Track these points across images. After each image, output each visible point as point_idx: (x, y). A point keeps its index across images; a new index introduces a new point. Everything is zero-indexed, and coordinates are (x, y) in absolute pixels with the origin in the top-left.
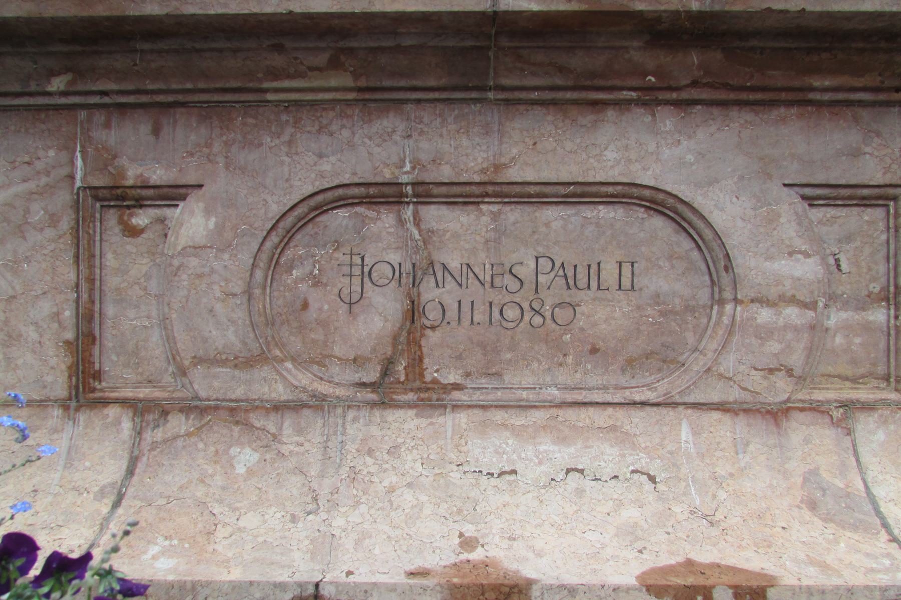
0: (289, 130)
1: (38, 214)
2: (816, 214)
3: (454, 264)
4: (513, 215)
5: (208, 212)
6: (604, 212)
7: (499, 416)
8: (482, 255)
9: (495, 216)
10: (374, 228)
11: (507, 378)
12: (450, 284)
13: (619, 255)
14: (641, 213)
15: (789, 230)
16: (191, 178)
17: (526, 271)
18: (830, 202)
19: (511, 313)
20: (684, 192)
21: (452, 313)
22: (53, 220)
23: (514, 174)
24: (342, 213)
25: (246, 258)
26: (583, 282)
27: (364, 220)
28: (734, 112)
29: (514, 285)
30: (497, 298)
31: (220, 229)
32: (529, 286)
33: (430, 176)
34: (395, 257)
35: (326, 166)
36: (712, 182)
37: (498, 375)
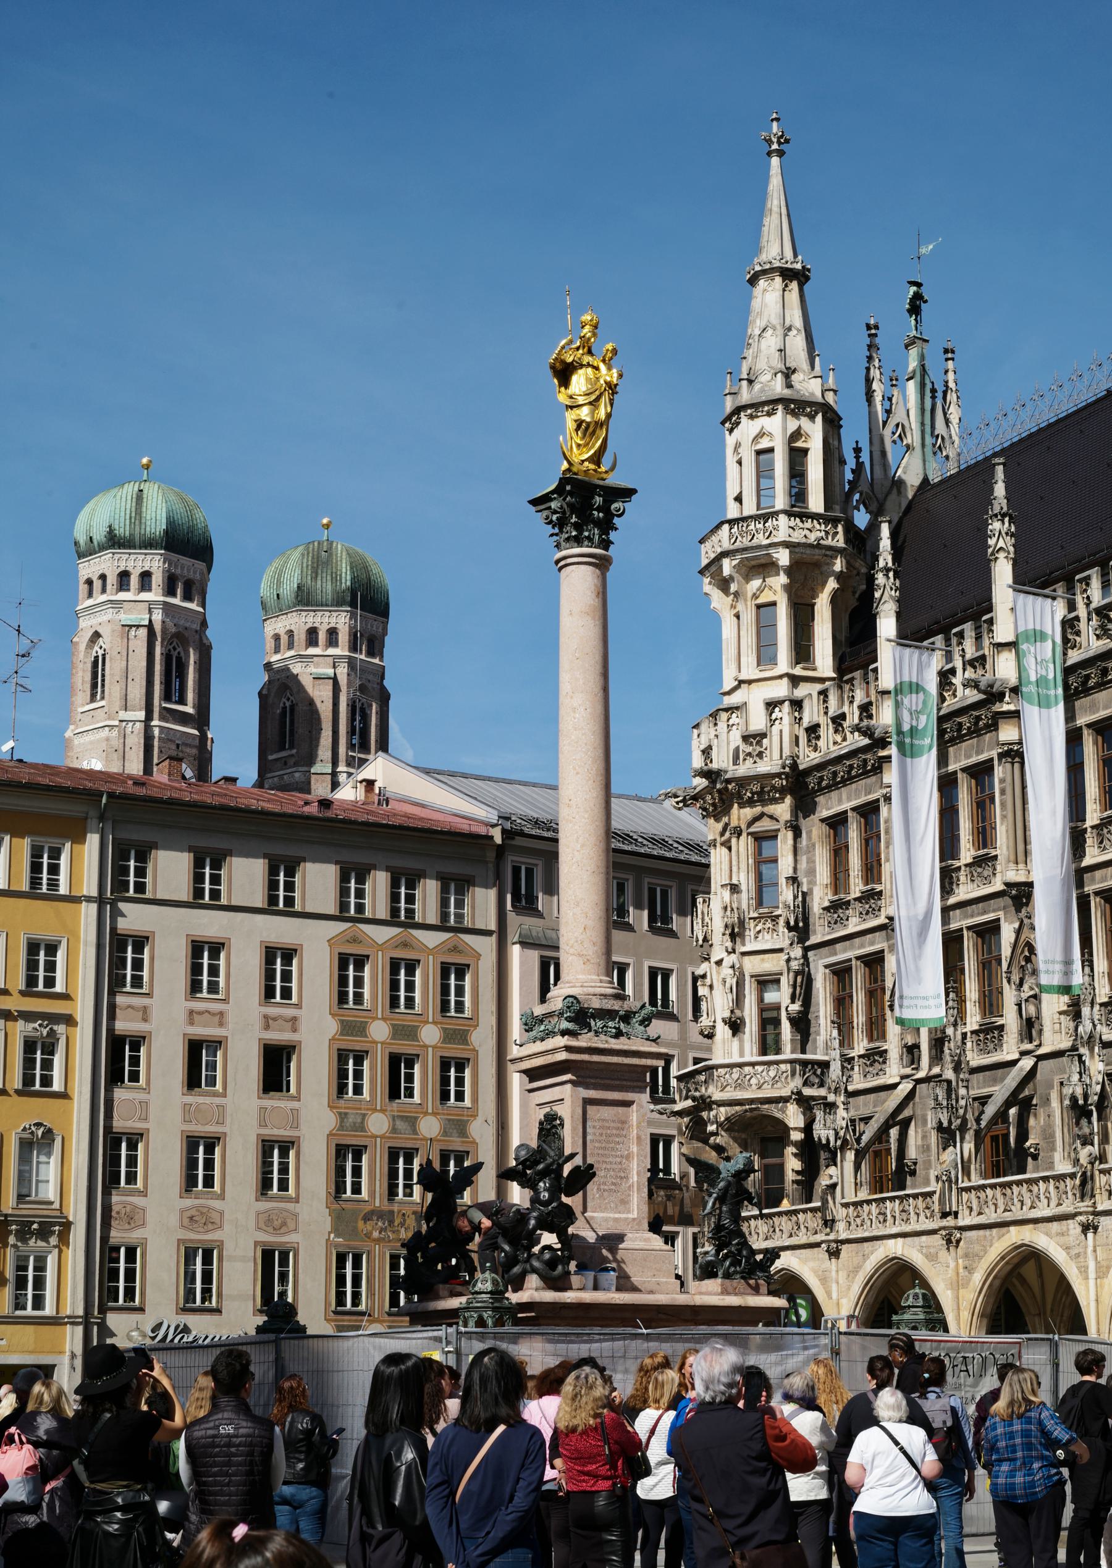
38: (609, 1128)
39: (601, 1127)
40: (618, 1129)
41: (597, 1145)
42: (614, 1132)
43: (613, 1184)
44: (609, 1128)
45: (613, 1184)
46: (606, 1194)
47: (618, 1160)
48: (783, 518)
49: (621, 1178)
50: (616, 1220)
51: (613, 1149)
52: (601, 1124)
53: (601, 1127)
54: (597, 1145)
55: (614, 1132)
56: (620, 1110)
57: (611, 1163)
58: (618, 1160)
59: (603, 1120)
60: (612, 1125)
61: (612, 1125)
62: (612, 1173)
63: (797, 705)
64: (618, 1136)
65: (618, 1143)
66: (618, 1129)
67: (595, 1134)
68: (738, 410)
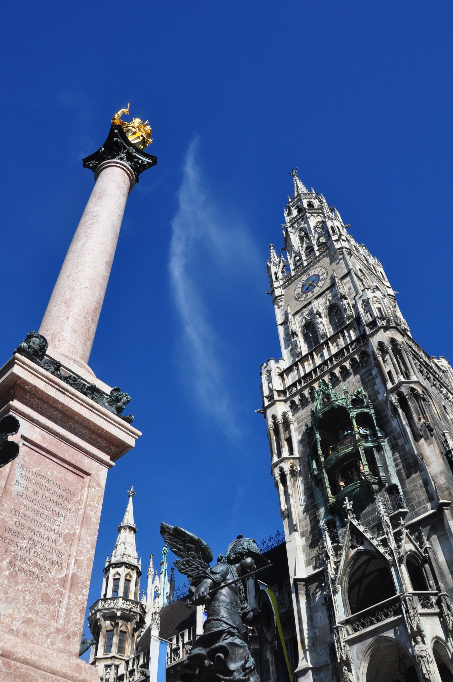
38: (49, 490)
43: (36, 565)
44: (49, 490)
45: (36, 565)
46: (21, 576)
48: (120, 599)
50: (28, 622)
52: (39, 480)
55: (56, 498)
56: (71, 477)
58: (54, 536)
59: (42, 477)
61: (55, 488)
63: (117, 667)
67: (27, 488)
68: (110, 565)
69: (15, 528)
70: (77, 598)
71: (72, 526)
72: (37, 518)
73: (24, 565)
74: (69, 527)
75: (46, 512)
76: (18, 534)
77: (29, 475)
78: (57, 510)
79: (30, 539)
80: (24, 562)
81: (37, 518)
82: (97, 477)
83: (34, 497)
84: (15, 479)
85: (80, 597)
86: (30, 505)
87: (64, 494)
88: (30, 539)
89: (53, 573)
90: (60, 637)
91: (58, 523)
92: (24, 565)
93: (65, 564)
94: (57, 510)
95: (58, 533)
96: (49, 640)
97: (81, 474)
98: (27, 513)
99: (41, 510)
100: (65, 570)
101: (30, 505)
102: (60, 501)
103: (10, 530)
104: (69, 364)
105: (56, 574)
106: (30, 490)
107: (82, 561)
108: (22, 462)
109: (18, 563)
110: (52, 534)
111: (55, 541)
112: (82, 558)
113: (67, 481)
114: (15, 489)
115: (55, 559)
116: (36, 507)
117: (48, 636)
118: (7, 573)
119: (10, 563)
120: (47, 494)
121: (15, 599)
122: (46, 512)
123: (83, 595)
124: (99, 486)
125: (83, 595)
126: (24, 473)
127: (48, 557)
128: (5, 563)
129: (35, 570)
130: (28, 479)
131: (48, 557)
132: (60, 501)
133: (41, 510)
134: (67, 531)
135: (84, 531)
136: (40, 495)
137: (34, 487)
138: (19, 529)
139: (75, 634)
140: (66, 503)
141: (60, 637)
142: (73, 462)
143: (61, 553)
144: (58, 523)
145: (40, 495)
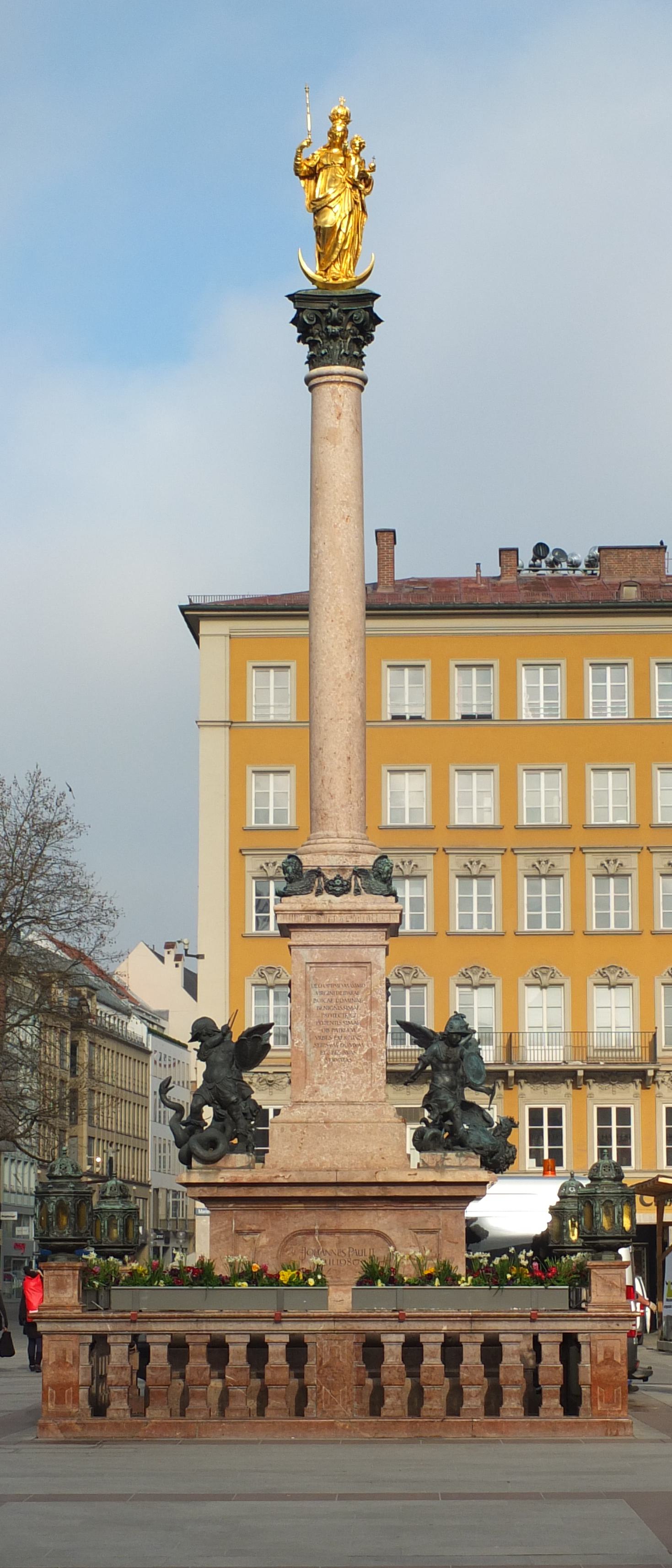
0: (287, 1217)
1: (223, 1237)
2: (418, 1236)
3: (328, 1250)
4: (342, 1236)
5: (267, 1237)
6: (365, 1236)
7: (340, 1288)
8: (335, 1248)
9: (339, 1237)
10: (308, 1240)
11: (342, 1279)
12: (327, 1255)
13: (369, 1247)
14: (375, 1236)
15: (410, 1240)
16: (262, 1228)
17: (347, 1251)
18: (422, 1233)
19: (343, 1262)
20: (385, 1232)
21: (328, 1262)
22: (227, 1239)
23: (343, 1227)
24: (300, 1237)
25: (277, 1248)
26: (360, 1254)
27: (306, 1238)
28: (397, 1211)
29: (343, 1255)
30: (339, 1258)
31: (270, 1241)
32: (347, 1255)
33: (323, 1228)
34: (313, 1248)
35: (296, 1225)
36: (391, 1229)
37: (339, 1278)
38: (340, 993)
39: (329, 993)
40: (351, 993)
41: (325, 1012)
42: (347, 997)
43: (344, 1052)
44: (340, 993)
47: (352, 1026)
49: (355, 1046)
51: (345, 1015)
53: (333, 993)
54: (325, 1012)
55: (347, 997)
56: (355, 972)
57: (342, 1030)
58: (352, 1026)
59: (333, 985)
60: (344, 989)
61: (344, 989)
62: (344, 1041)
64: (349, 1001)
65: (352, 1008)
66: (351, 993)
67: (323, 1000)
69: (323, 1034)
70: (377, 1064)
71: (365, 1012)
72: (336, 1019)
73: (336, 1056)
74: (363, 1014)
75: (342, 1012)
76: (326, 1038)
77: (321, 990)
78: (350, 1005)
79: (335, 1037)
80: (335, 1054)
81: (336, 1019)
82: (376, 961)
83: (330, 1005)
84: (313, 998)
85: (380, 1063)
86: (329, 1012)
87: (353, 989)
88: (335, 1037)
89: (358, 1052)
90: (370, 1093)
91: (353, 1015)
92: (336, 1056)
93: (365, 1043)
94: (350, 1005)
95: (356, 1023)
96: (363, 1097)
97: (363, 965)
98: (328, 1019)
99: (338, 1012)
100: (366, 1046)
101: (329, 1012)
102: (351, 997)
103: (320, 1037)
104: (328, 860)
105: (360, 1051)
106: (326, 1001)
107: (376, 1037)
108: (314, 983)
109: (331, 1056)
110: (350, 1025)
111: (354, 1030)
112: (376, 1035)
113: (352, 976)
114: (315, 1005)
115: (356, 1042)
116: (333, 1012)
117: (361, 1095)
118: (326, 1066)
119: (326, 1059)
120: (340, 997)
121: (336, 1078)
122: (342, 1012)
123: (382, 1060)
124: (380, 968)
125: (382, 1060)
126: (317, 990)
127: (352, 1043)
128: (322, 1060)
129: (345, 1056)
130: (322, 993)
131: (352, 1043)
132: (351, 997)
133: (338, 1012)
134: (361, 1018)
135: (374, 1013)
136: (334, 1001)
137: (328, 997)
138: (326, 1034)
139: (380, 1088)
140: (356, 996)
141: (370, 1093)
142: (353, 961)
143: (360, 1036)
144: (353, 1015)
145: (334, 1001)
